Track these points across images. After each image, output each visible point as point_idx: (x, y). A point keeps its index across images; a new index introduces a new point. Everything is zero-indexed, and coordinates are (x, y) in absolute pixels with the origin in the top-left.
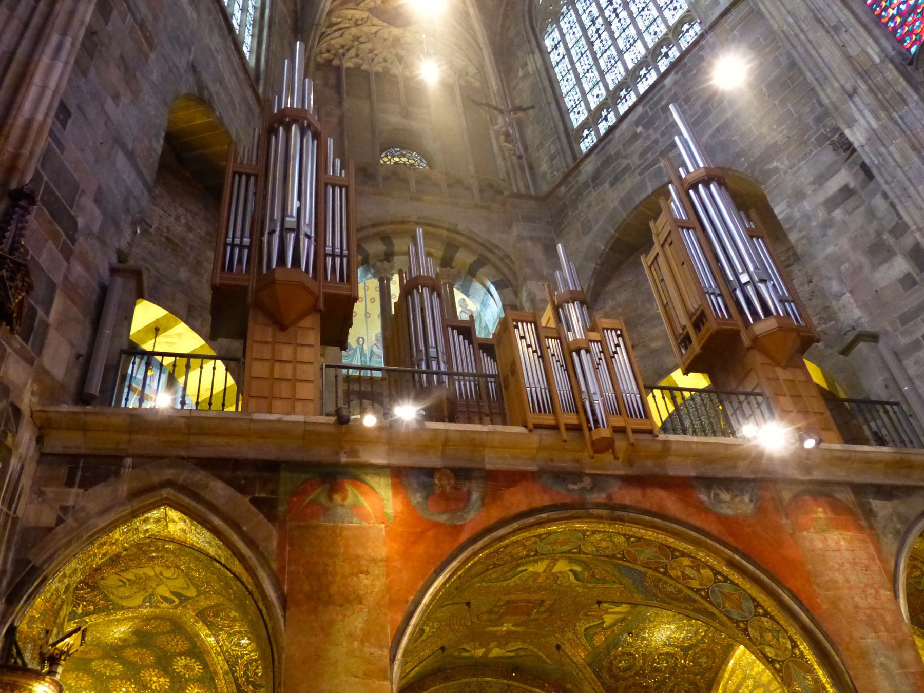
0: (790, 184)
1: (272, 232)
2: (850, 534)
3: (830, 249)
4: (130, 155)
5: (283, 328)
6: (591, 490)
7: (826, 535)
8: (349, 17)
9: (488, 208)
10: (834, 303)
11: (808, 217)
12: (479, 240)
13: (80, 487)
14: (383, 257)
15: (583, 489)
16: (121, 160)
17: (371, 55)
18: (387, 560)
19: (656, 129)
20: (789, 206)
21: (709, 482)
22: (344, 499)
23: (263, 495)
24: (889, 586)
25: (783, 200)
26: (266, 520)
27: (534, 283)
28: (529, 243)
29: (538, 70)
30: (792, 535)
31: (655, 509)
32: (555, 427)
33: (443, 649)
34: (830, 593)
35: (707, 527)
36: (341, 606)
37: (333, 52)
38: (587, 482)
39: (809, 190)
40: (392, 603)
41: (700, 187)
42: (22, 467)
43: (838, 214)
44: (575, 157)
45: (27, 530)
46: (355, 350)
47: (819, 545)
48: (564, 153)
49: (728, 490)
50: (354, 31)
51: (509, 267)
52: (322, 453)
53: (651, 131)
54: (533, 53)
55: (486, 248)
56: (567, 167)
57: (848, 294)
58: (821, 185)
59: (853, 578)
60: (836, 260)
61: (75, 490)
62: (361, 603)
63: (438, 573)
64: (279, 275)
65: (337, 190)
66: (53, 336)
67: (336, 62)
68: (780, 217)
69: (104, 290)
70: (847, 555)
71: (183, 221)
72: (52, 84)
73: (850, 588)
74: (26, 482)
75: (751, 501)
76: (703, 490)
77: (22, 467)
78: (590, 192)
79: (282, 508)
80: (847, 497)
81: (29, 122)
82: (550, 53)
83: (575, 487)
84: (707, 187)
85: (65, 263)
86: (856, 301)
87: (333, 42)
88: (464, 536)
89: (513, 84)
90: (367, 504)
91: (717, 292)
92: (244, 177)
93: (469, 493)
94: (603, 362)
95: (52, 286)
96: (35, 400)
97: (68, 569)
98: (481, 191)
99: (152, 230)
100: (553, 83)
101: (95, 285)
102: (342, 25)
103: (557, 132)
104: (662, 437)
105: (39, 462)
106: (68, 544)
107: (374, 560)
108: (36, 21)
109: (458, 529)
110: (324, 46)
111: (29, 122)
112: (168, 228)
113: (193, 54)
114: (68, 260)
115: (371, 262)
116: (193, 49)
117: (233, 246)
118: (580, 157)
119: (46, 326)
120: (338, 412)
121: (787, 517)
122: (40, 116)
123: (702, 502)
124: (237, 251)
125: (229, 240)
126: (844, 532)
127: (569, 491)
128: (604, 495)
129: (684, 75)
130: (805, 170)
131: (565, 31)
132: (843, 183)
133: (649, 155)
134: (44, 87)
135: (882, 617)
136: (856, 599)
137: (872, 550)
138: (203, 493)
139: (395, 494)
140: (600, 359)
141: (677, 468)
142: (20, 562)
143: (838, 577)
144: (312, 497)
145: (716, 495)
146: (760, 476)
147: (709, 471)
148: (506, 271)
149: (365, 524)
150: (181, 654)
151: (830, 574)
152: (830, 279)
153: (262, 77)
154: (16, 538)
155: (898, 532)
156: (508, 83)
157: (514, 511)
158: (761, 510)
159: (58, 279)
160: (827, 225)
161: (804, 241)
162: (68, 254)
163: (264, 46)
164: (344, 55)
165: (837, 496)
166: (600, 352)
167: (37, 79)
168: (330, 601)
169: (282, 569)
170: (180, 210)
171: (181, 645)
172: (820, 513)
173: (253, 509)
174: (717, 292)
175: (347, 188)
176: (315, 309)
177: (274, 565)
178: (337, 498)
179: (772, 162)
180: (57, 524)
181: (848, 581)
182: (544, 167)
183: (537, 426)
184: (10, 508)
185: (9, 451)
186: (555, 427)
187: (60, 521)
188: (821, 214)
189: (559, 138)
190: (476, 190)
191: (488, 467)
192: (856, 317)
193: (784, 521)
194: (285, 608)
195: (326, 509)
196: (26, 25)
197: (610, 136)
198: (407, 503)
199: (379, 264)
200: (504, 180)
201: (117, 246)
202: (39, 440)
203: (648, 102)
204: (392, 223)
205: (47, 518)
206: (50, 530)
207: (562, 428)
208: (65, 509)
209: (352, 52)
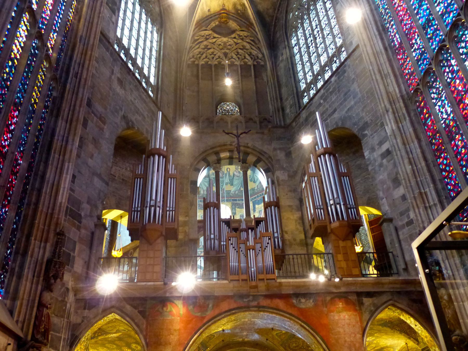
0: (370, 143)
1: (147, 207)
2: (351, 313)
3: (381, 177)
4: (99, 176)
5: (151, 244)
6: (252, 301)
7: (341, 314)
8: (203, 35)
9: (263, 133)
10: (380, 201)
11: (375, 160)
12: (258, 150)
13: (88, 309)
14: (216, 162)
15: (249, 301)
16: (96, 180)
17: (213, 56)
18: (179, 330)
19: (328, 102)
20: (370, 153)
21: (297, 295)
22: (167, 309)
23: (142, 309)
24: (361, 333)
25: (368, 150)
26: (142, 318)
27: (279, 172)
28: (278, 152)
29: (287, 58)
30: (326, 315)
31: (275, 307)
32: (239, 280)
33: (223, 341)
34: (336, 336)
35: (293, 313)
36: (164, 345)
37: (195, 57)
38: (251, 298)
39: (377, 147)
40: (180, 344)
41: (322, 156)
42: (71, 306)
43: (385, 161)
44: (300, 107)
45: (74, 325)
46: (226, 174)
47: (336, 318)
48: (296, 105)
49: (304, 298)
50: (205, 43)
51: (270, 162)
52: (160, 293)
53: (326, 103)
54: (286, 48)
55: (261, 154)
56: (297, 112)
57: (385, 199)
58: (380, 146)
59: (347, 330)
60: (383, 182)
61: (86, 311)
62: (170, 344)
63: (195, 334)
64: (148, 227)
65: (173, 179)
66: (77, 258)
67: (196, 63)
68: (366, 158)
69: (93, 233)
70: (347, 321)
71: (128, 169)
72: (67, 186)
73: (345, 334)
74: (72, 310)
75: (313, 302)
76: (295, 298)
77: (71, 306)
79: (147, 314)
80: (353, 298)
81: (61, 203)
82: (293, 47)
83: (246, 300)
84: (324, 156)
85: (79, 232)
86: (387, 203)
87: (195, 51)
88: (205, 321)
89: (277, 64)
90: (174, 311)
91: (322, 207)
92: (139, 179)
93: (208, 305)
94: (260, 252)
95: (75, 242)
96: (73, 283)
97: (86, 335)
98: (261, 122)
99: (116, 178)
100: (293, 65)
101: (89, 234)
102: (200, 40)
103: (293, 93)
104: (278, 281)
105: (76, 302)
106: (85, 328)
107: (175, 330)
108: (59, 166)
109: (203, 318)
110: (191, 55)
111: (61, 203)
112: (123, 175)
113: (123, 111)
114: (79, 231)
115: (211, 165)
116: (123, 109)
117: (134, 211)
118: (302, 107)
119: (74, 257)
120: (164, 281)
121: (326, 307)
122: (64, 201)
123: (293, 303)
124: (136, 213)
125: (133, 209)
126: (348, 312)
127: (244, 302)
128: (256, 303)
129: (339, 78)
130: (376, 138)
131: (299, 37)
132: (387, 148)
133: (324, 115)
134: (64, 188)
135: (355, 345)
136: (346, 338)
137: (358, 319)
138: (124, 310)
139: (184, 306)
140: (268, 243)
141: (285, 291)
142: (73, 335)
143: (341, 330)
144: (157, 309)
145: (300, 300)
146: (319, 292)
147: (298, 291)
148: (269, 165)
149: (173, 318)
150: (133, 343)
151: (338, 329)
152: (380, 190)
153: (160, 89)
154: (71, 327)
155: (371, 311)
156: (276, 63)
157: (224, 310)
158: (316, 305)
159: (76, 239)
160: (381, 165)
161: (373, 171)
162: (79, 228)
163: (160, 73)
164: (200, 57)
165: (349, 297)
167: (62, 186)
168: (160, 344)
169: (147, 334)
170: (127, 165)
171: (133, 341)
172: (340, 305)
173: (139, 314)
174: (322, 207)
175: (176, 178)
176: (162, 235)
177: (145, 333)
178: (165, 309)
179: (365, 131)
180: (82, 322)
181: (345, 331)
182: (288, 111)
183: (232, 280)
184: (68, 319)
185: (67, 302)
186: (239, 280)
187: (83, 321)
188: (379, 159)
189: (294, 97)
190: (258, 122)
191: (216, 294)
192: (386, 210)
193: (325, 309)
194: (147, 346)
195: (161, 313)
196: (57, 168)
197: (311, 102)
198: (187, 309)
199: (214, 165)
200: (271, 117)
201: (96, 214)
202: (75, 295)
203: (325, 88)
204: (219, 146)
205: (79, 321)
206: (80, 324)
207: (240, 280)
208: (84, 317)
209: (204, 56)
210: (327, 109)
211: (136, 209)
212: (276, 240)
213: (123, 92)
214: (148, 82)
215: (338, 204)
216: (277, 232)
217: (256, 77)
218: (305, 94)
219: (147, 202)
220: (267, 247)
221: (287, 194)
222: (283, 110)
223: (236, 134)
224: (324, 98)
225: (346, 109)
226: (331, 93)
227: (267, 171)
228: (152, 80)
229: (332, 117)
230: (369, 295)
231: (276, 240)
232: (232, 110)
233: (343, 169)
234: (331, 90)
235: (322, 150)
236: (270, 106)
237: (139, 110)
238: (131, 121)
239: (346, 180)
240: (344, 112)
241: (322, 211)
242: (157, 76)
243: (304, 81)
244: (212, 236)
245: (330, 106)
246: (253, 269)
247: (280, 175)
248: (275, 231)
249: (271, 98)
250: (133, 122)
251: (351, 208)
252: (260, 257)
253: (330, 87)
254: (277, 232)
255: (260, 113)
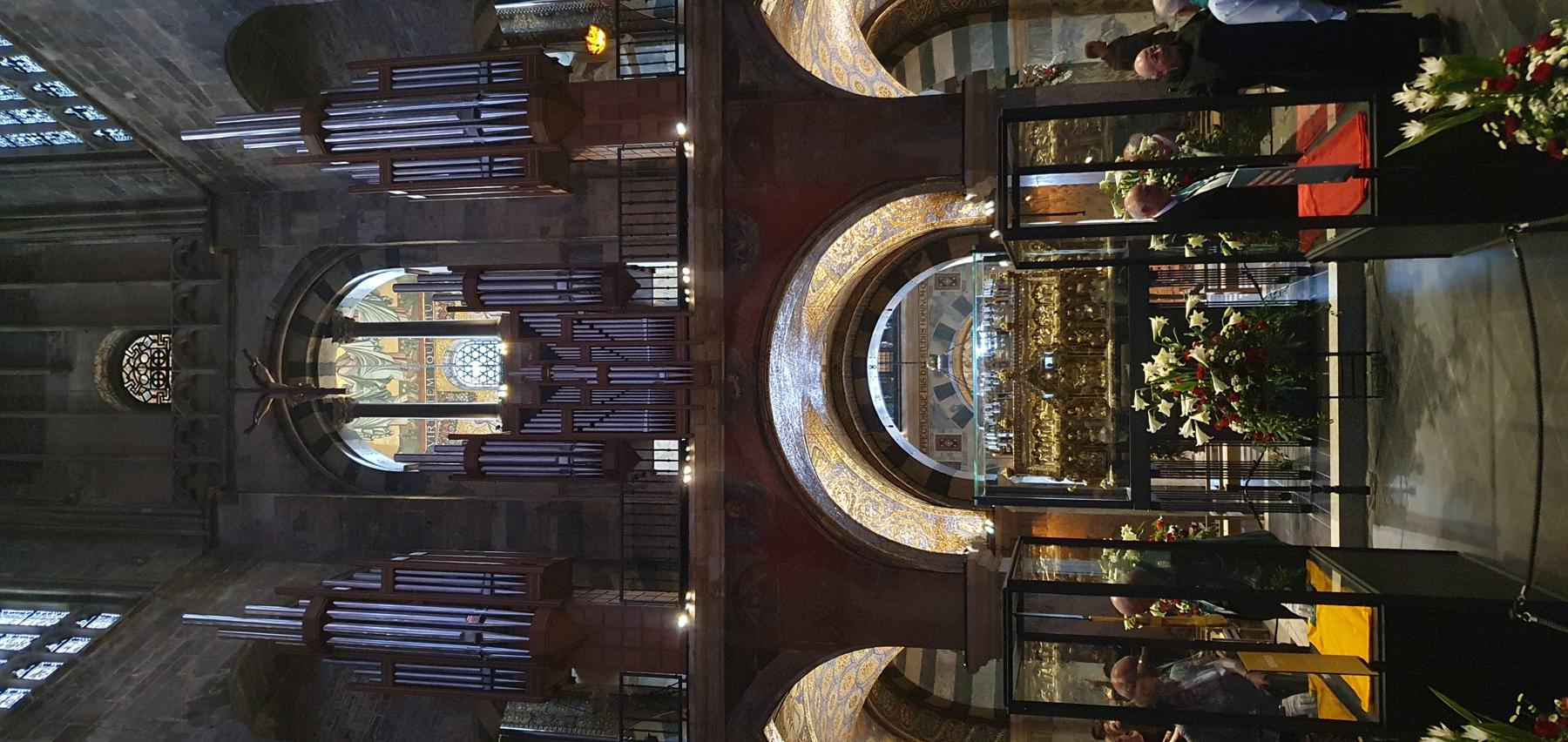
1: (481, 653)
28: (294, 231)
48: (136, 167)
53: (137, 85)
78: (219, 153)
91: (486, 159)
94: (617, 349)
98: (195, 275)
125: (487, 688)
148: (335, 261)
166: (603, 349)
189: (105, 168)
200: (175, 240)
203: (83, 81)
210: (160, 84)
211: (487, 680)
212: (575, 286)
213: (106, 723)
214: (61, 633)
215: (477, 115)
216: (554, 282)
217: (28, 277)
218: (98, 133)
219: (467, 652)
220: (601, 330)
221: (431, 218)
222: (154, 203)
223: (257, 396)
224: (118, 86)
225: (164, 33)
226: (102, 66)
227: (358, 265)
228: (49, 618)
229: (189, 74)
230: (730, 67)
231: (575, 286)
232: (152, 358)
233: (371, 80)
234: (91, 66)
235: (311, 139)
236: (140, 239)
237: (163, 666)
238: (205, 689)
239: (402, 76)
240: (175, 41)
241: (496, 160)
242: (33, 603)
243: (48, 135)
244: (563, 460)
245: (150, 75)
246: (662, 375)
247: (368, 235)
248: (551, 287)
249: (110, 237)
250: (210, 684)
251: (490, 76)
252: (628, 352)
253: (78, 67)
254: (554, 282)
255: (164, 276)
